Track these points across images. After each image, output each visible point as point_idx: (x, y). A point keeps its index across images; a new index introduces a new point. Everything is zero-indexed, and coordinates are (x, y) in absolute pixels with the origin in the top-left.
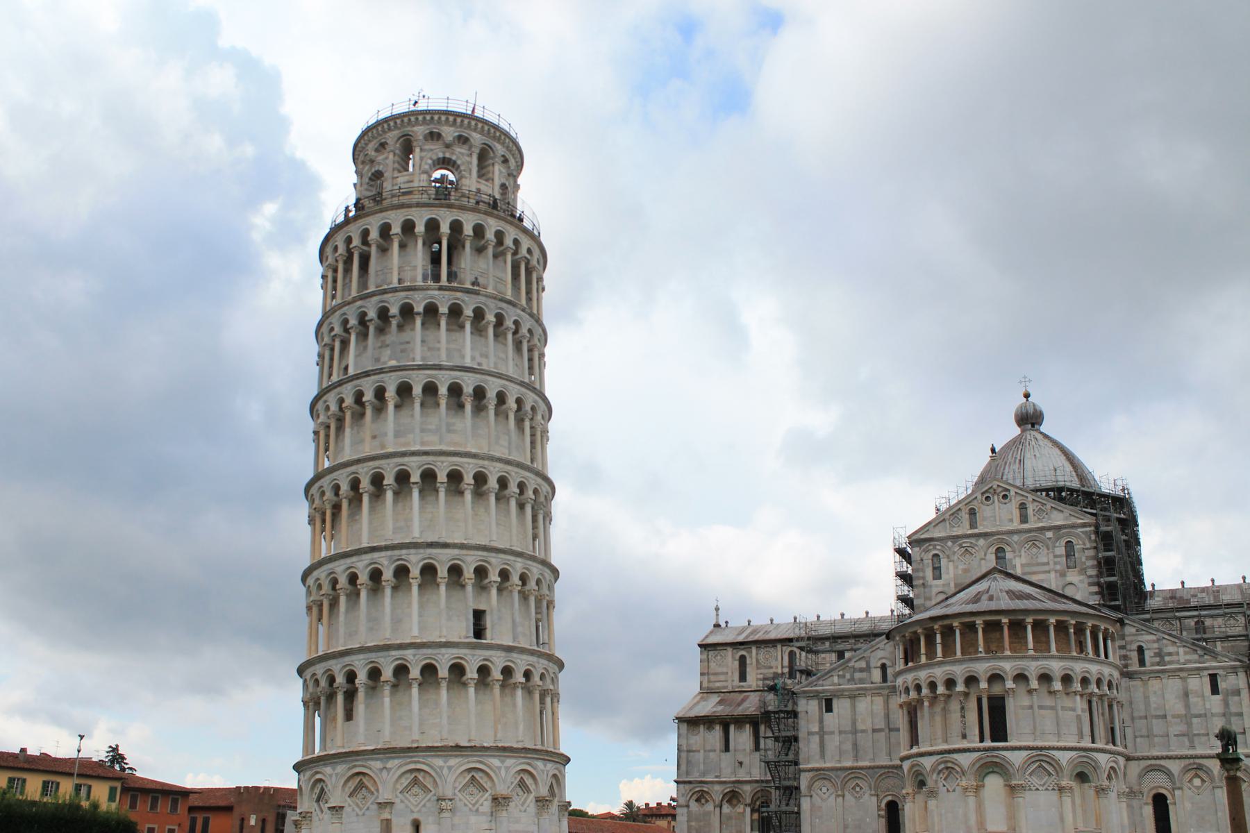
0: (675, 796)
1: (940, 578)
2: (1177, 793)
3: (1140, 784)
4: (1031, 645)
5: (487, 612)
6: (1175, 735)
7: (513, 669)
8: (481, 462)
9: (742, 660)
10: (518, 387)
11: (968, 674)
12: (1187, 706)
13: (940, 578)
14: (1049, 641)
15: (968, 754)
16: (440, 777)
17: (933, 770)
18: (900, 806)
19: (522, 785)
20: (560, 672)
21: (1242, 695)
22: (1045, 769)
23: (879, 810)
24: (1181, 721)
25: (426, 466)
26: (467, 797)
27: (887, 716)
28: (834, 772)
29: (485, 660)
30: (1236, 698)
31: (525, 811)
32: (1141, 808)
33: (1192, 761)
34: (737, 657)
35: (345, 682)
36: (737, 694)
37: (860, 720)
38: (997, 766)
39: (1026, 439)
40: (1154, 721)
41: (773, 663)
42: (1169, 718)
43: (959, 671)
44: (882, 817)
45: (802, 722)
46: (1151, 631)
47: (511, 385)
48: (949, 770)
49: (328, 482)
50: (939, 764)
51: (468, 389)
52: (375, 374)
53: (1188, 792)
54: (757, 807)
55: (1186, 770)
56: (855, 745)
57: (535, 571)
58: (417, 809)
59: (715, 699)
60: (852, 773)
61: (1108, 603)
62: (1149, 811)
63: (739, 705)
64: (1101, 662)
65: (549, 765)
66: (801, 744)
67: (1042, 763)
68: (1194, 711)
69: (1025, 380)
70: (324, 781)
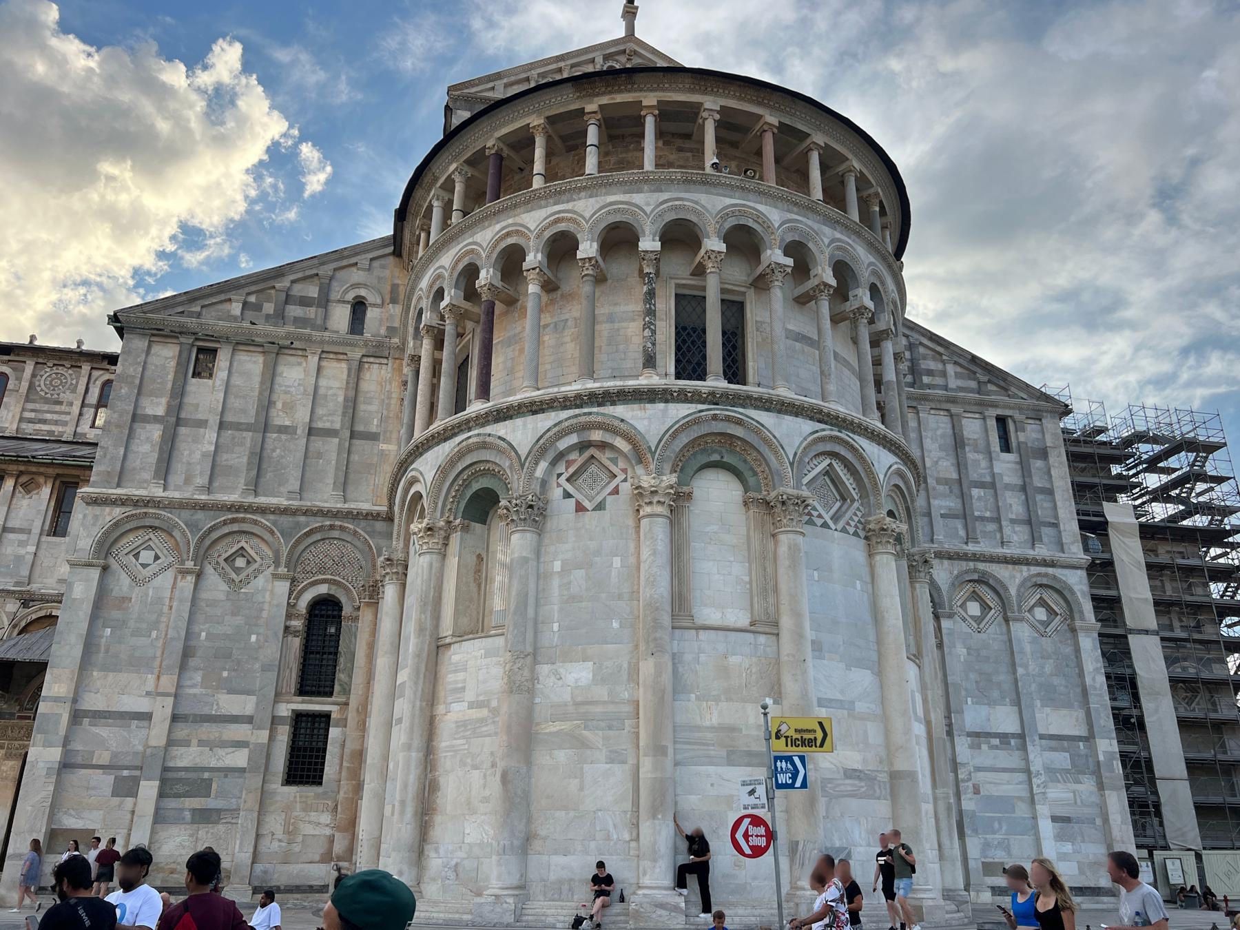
11: (672, 216)
15: (661, 406)
17: (541, 449)
18: (347, 610)
21: (1051, 460)
23: (289, 616)
24: (951, 492)
28: (186, 514)
30: (1039, 463)
33: (971, 564)
37: (279, 405)
41: (66, 396)
55: (959, 582)
56: (259, 460)
60: (234, 521)
67: (833, 462)
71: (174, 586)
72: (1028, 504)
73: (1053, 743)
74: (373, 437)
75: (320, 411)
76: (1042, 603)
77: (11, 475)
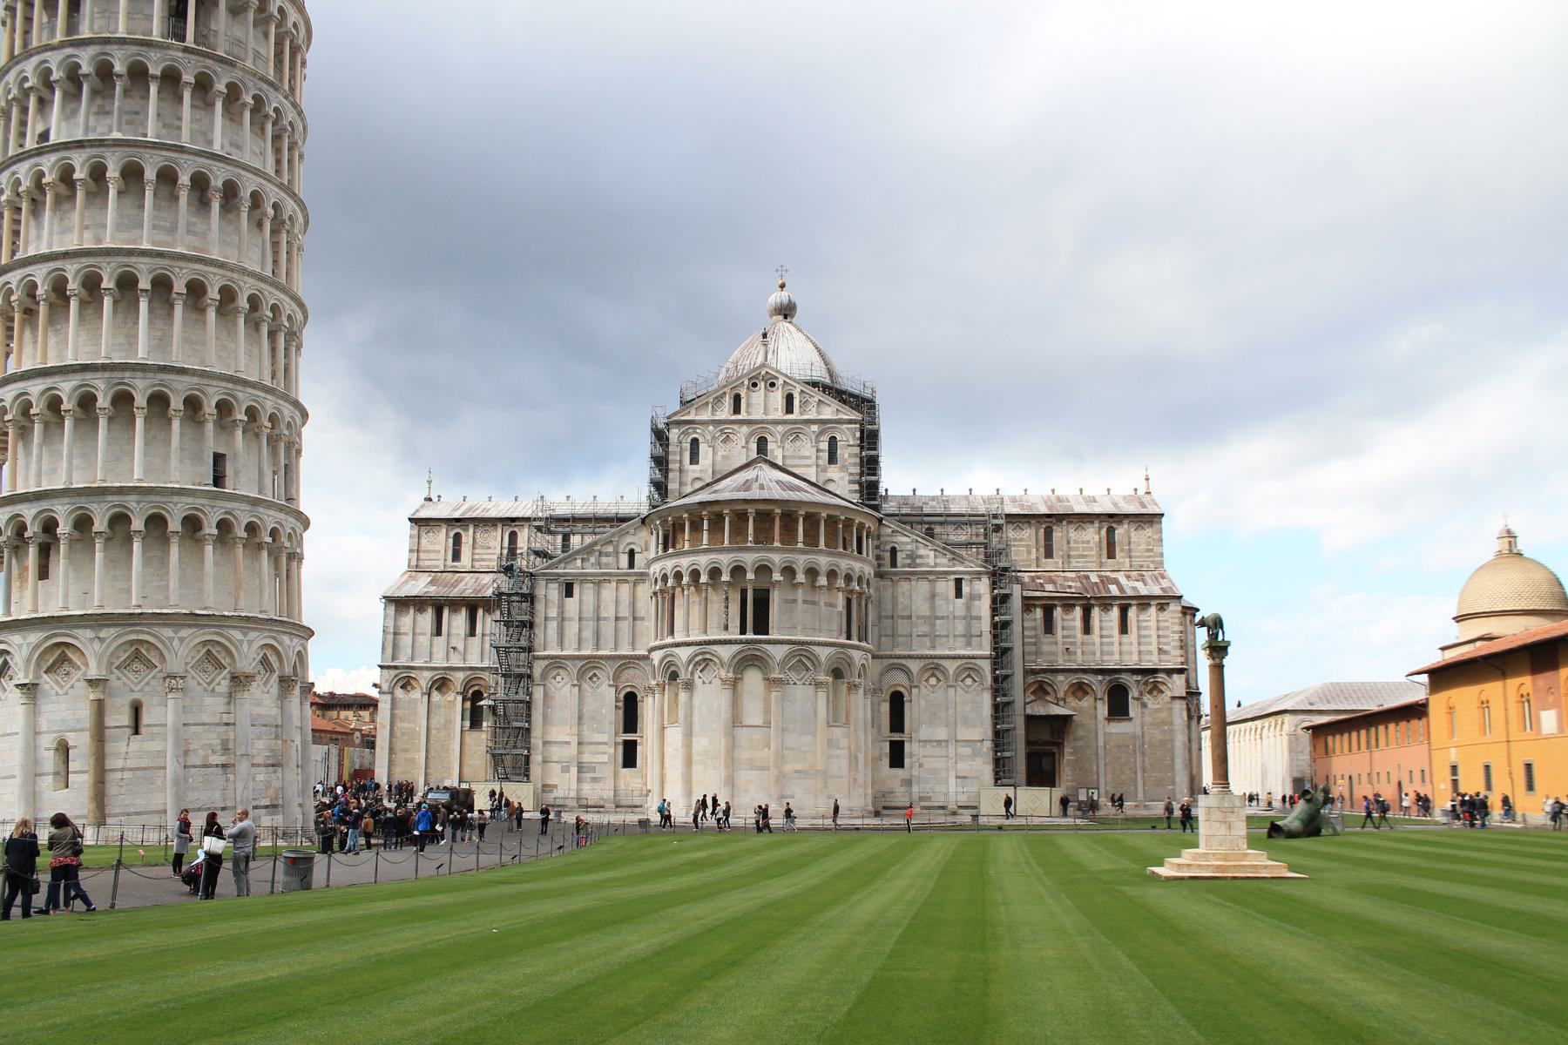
0: (378, 682)
1: (697, 463)
2: (915, 691)
3: (881, 682)
4: (801, 538)
5: (227, 457)
6: (918, 636)
7: (258, 526)
8: (229, 274)
9: (457, 539)
10: (277, 190)
12: (933, 608)
13: (697, 463)
14: (818, 536)
16: (169, 651)
18: (639, 698)
19: (264, 661)
20: (305, 530)
22: (803, 664)
23: (617, 701)
25: (159, 271)
26: (201, 674)
27: (633, 603)
29: (226, 513)
31: (267, 693)
32: (879, 704)
33: (931, 661)
34: (452, 534)
35: (41, 531)
36: (450, 575)
37: (602, 607)
38: (757, 660)
39: (779, 330)
40: (900, 621)
41: (492, 544)
42: (914, 619)
43: (725, 560)
44: (620, 708)
45: (540, 606)
46: (906, 533)
47: (269, 187)
48: (704, 663)
49: (18, 277)
50: (696, 655)
51: (217, 182)
52: (92, 146)
53: (924, 691)
54: (469, 695)
55: (924, 670)
56: (597, 635)
57: (287, 411)
58: (139, 687)
59: (426, 578)
61: (867, 502)
62: (885, 707)
63: (454, 585)
64: (863, 561)
65: (296, 640)
66: (539, 631)
68: (939, 614)
69: (782, 270)
70: (8, 652)
71: (571, 691)
72: (968, 627)
73: (964, 744)
74: (642, 619)
75: (620, 608)
76: (969, 676)
77: (481, 606)
